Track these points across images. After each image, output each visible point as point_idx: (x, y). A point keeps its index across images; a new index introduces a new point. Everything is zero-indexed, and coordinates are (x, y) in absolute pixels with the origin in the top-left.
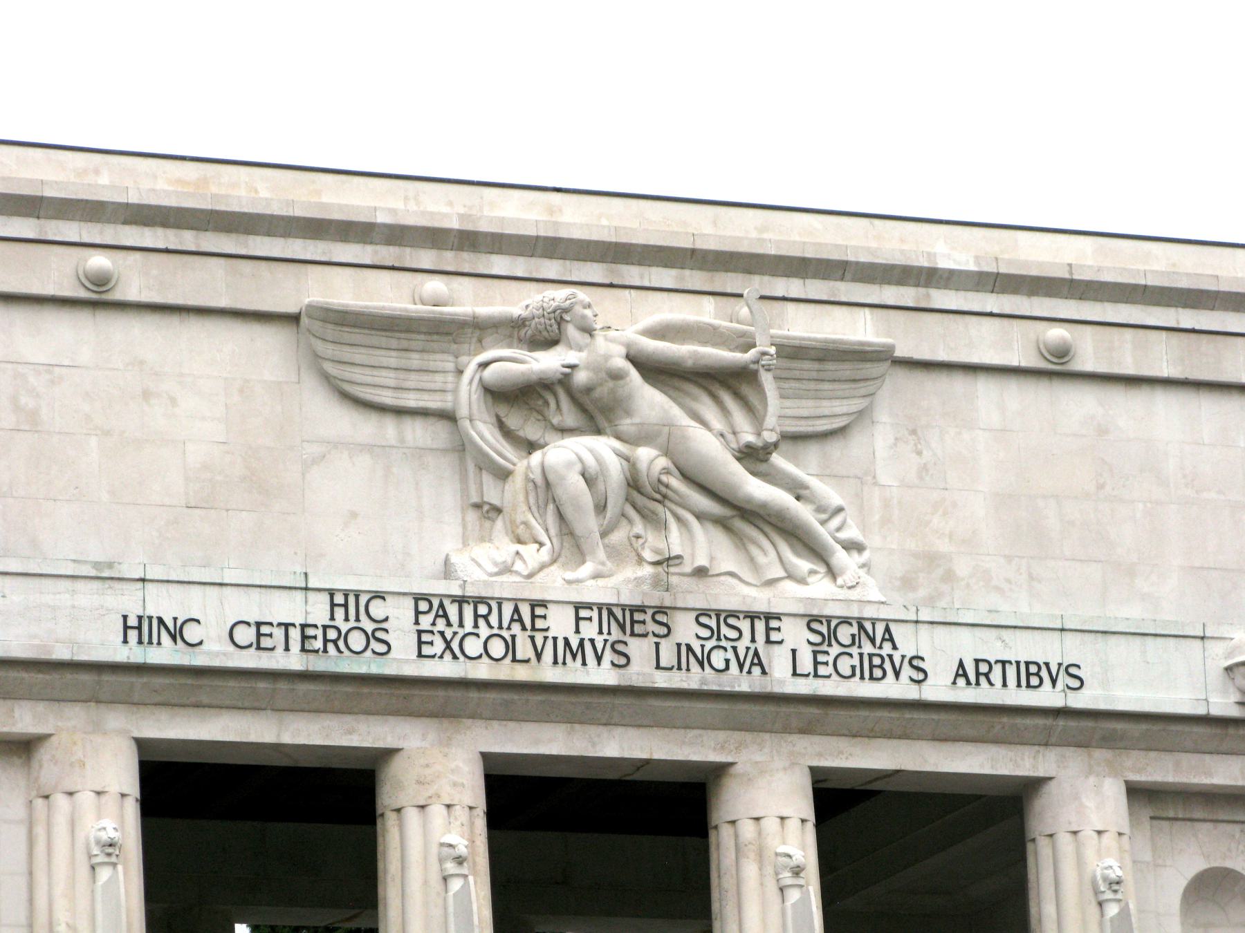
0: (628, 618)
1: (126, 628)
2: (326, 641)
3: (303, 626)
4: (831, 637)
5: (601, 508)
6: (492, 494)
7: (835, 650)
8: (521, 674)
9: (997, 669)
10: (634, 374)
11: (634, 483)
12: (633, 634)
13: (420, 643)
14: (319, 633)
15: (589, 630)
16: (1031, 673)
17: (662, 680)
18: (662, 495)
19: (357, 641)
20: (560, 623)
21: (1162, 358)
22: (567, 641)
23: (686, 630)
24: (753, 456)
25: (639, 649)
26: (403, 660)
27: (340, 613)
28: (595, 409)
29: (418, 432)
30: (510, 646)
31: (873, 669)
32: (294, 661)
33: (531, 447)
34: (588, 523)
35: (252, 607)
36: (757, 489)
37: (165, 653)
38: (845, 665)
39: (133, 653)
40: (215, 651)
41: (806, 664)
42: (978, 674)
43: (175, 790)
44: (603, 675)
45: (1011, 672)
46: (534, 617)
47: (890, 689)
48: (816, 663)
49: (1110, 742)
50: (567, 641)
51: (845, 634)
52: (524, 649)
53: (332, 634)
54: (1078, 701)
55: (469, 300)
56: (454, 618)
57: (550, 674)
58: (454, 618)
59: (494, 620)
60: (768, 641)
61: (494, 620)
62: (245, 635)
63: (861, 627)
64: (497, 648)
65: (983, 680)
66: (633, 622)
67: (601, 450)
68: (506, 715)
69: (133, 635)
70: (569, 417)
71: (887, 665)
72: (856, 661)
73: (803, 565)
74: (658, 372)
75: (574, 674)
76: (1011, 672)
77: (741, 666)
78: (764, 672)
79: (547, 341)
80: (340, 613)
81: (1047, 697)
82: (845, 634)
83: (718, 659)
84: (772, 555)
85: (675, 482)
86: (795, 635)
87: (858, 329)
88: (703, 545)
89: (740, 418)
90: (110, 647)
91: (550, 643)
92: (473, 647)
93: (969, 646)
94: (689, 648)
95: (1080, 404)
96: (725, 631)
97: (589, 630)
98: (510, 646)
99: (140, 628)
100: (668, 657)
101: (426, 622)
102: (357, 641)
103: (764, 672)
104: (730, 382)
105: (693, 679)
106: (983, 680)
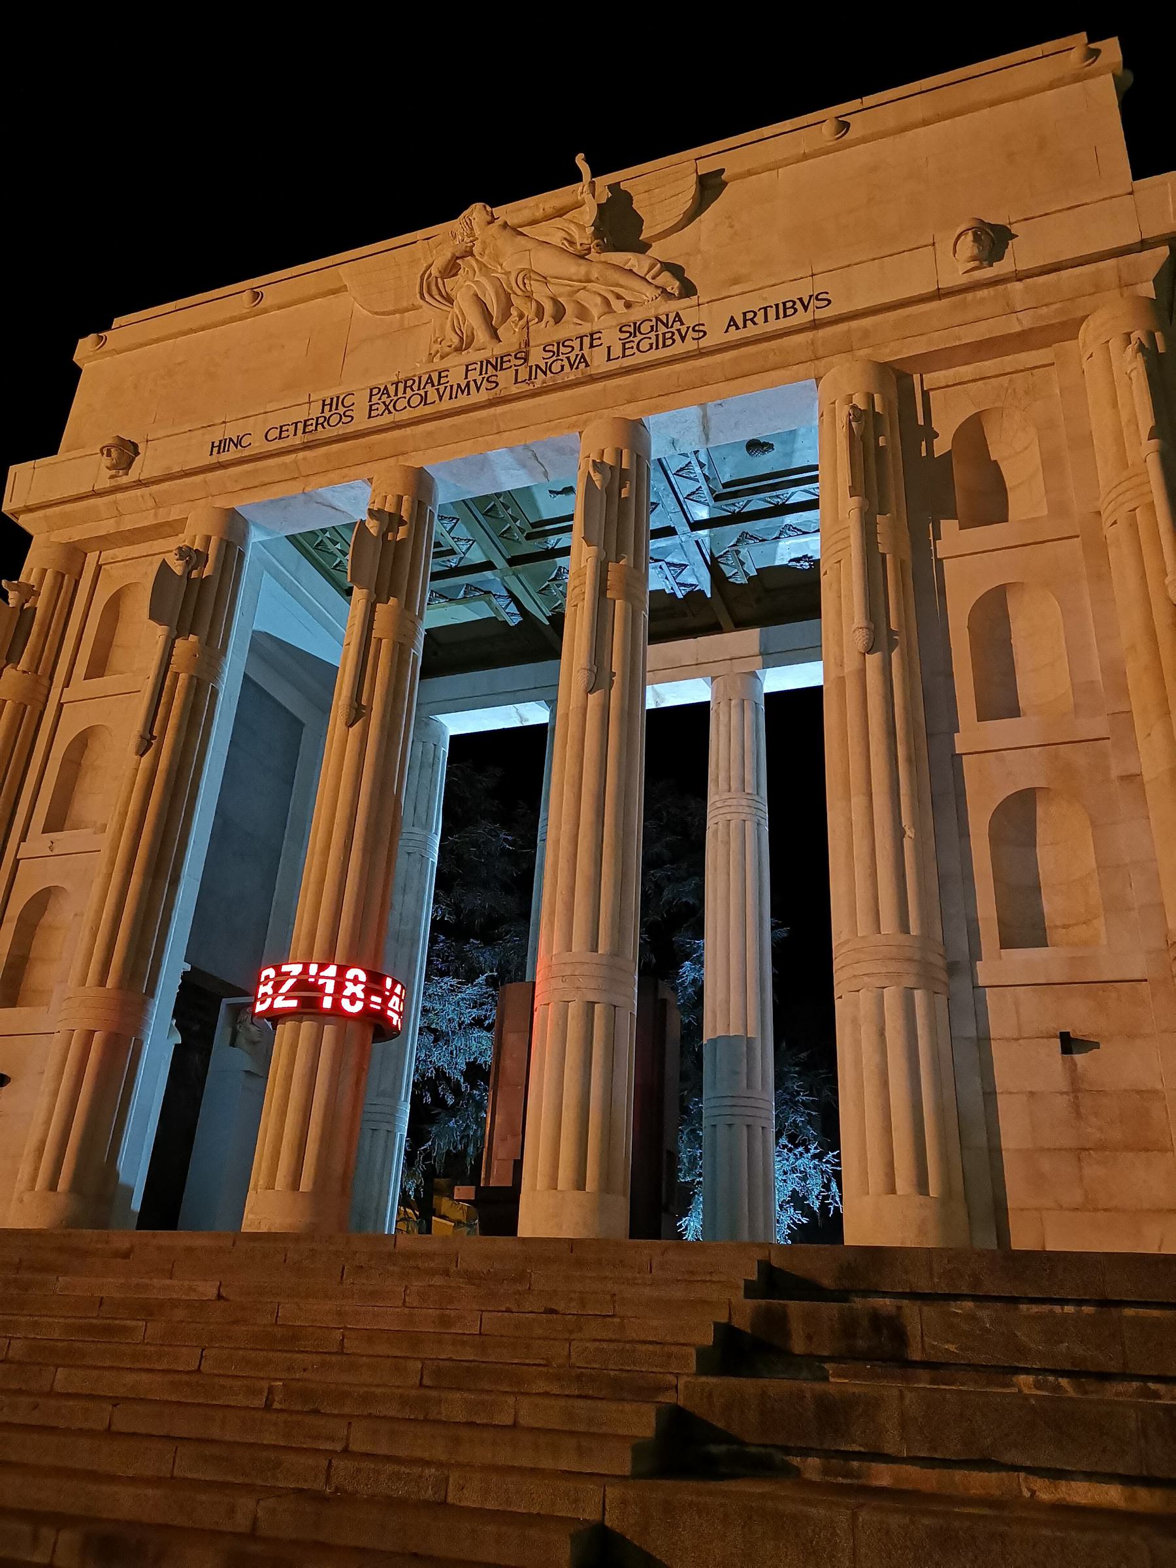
1: (213, 447)
2: (317, 424)
3: (306, 421)
7: (639, 337)
9: (761, 313)
12: (502, 369)
13: (371, 410)
14: (314, 422)
17: (514, 389)
20: (456, 377)
22: (459, 386)
23: (537, 357)
25: (504, 377)
27: (327, 408)
30: (424, 400)
32: (298, 440)
35: (276, 420)
37: (232, 454)
38: (644, 345)
41: (617, 351)
42: (745, 321)
45: (772, 313)
46: (440, 377)
47: (679, 348)
48: (624, 349)
50: (459, 386)
51: (645, 328)
52: (432, 396)
53: (321, 420)
56: (392, 393)
57: (446, 405)
58: (392, 393)
59: (415, 387)
60: (592, 346)
61: (415, 387)
62: (274, 434)
63: (658, 319)
64: (416, 400)
65: (749, 323)
66: (502, 363)
69: (215, 450)
71: (677, 337)
72: (653, 340)
76: (772, 313)
77: (571, 366)
78: (587, 365)
80: (327, 408)
83: (556, 368)
91: (448, 389)
94: (537, 366)
96: (562, 349)
98: (424, 400)
99: (221, 446)
100: (523, 374)
101: (375, 399)
103: (587, 365)
106: (749, 323)
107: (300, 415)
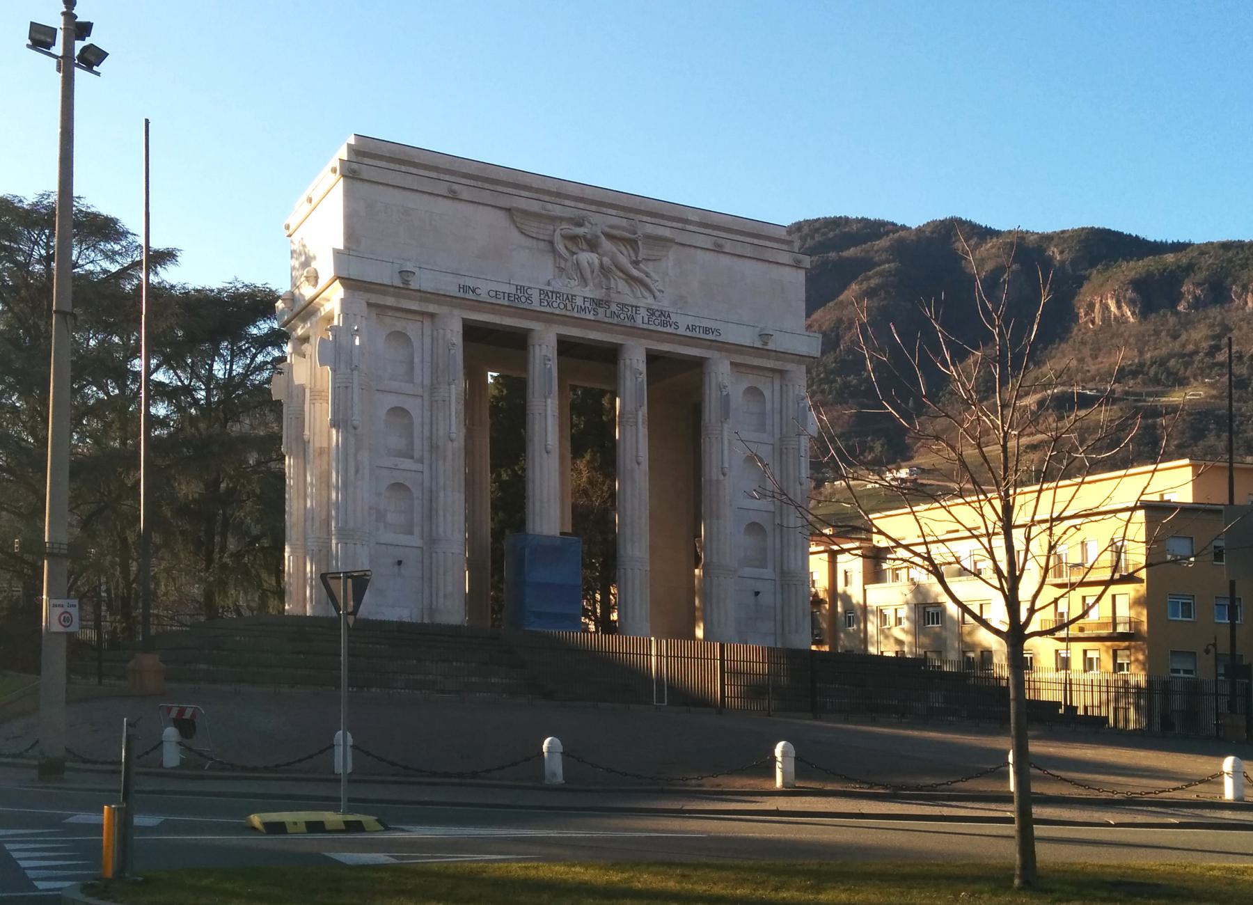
0: (598, 303)
4: (653, 314)
5: (593, 272)
6: (563, 264)
8: (568, 313)
10: (603, 237)
11: (602, 266)
15: (587, 304)
16: (706, 330)
17: (606, 320)
18: (610, 271)
19: (523, 299)
20: (579, 301)
21: (749, 251)
23: (614, 308)
24: (636, 263)
25: (601, 311)
26: (536, 305)
28: (593, 245)
29: (542, 245)
30: (565, 306)
31: (663, 324)
32: (506, 302)
33: (574, 253)
34: (588, 275)
35: (495, 286)
36: (635, 273)
37: (470, 296)
39: (461, 295)
40: (484, 297)
41: (646, 320)
43: (472, 332)
44: (591, 317)
49: (727, 350)
51: (657, 314)
52: (569, 307)
54: (719, 339)
55: (557, 210)
57: (576, 315)
62: (493, 294)
67: (594, 258)
68: (564, 324)
70: (585, 246)
73: (647, 294)
74: (610, 237)
75: (582, 315)
79: (581, 225)
81: (710, 337)
82: (657, 314)
84: (639, 291)
85: (614, 268)
86: (643, 312)
87: (667, 233)
88: (622, 285)
89: (632, 254)
90: (454, 291)
92: (555, 305)
93: (690, 321)
95: (725, 260)
97: (587, 304)
98: (565, 306)
99: (465, 288)
102: (523, 299)
104: (632, 243)
105: (615, 321)
107: (506, 289)
